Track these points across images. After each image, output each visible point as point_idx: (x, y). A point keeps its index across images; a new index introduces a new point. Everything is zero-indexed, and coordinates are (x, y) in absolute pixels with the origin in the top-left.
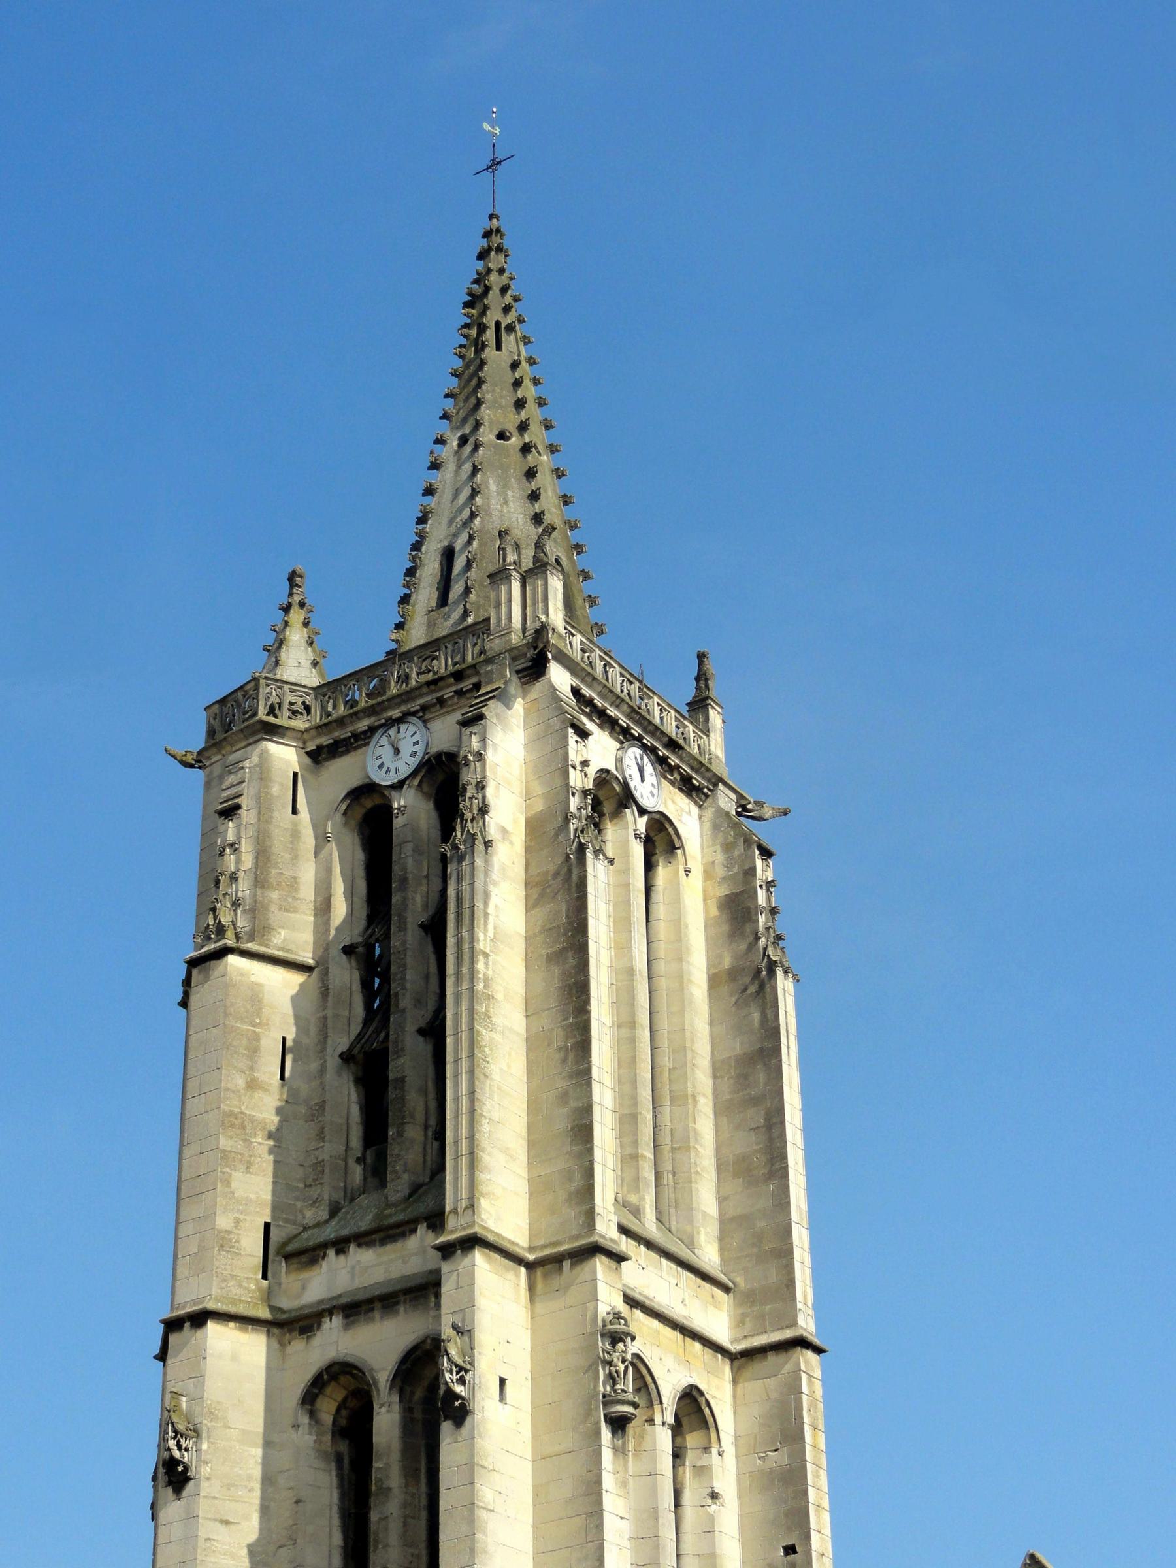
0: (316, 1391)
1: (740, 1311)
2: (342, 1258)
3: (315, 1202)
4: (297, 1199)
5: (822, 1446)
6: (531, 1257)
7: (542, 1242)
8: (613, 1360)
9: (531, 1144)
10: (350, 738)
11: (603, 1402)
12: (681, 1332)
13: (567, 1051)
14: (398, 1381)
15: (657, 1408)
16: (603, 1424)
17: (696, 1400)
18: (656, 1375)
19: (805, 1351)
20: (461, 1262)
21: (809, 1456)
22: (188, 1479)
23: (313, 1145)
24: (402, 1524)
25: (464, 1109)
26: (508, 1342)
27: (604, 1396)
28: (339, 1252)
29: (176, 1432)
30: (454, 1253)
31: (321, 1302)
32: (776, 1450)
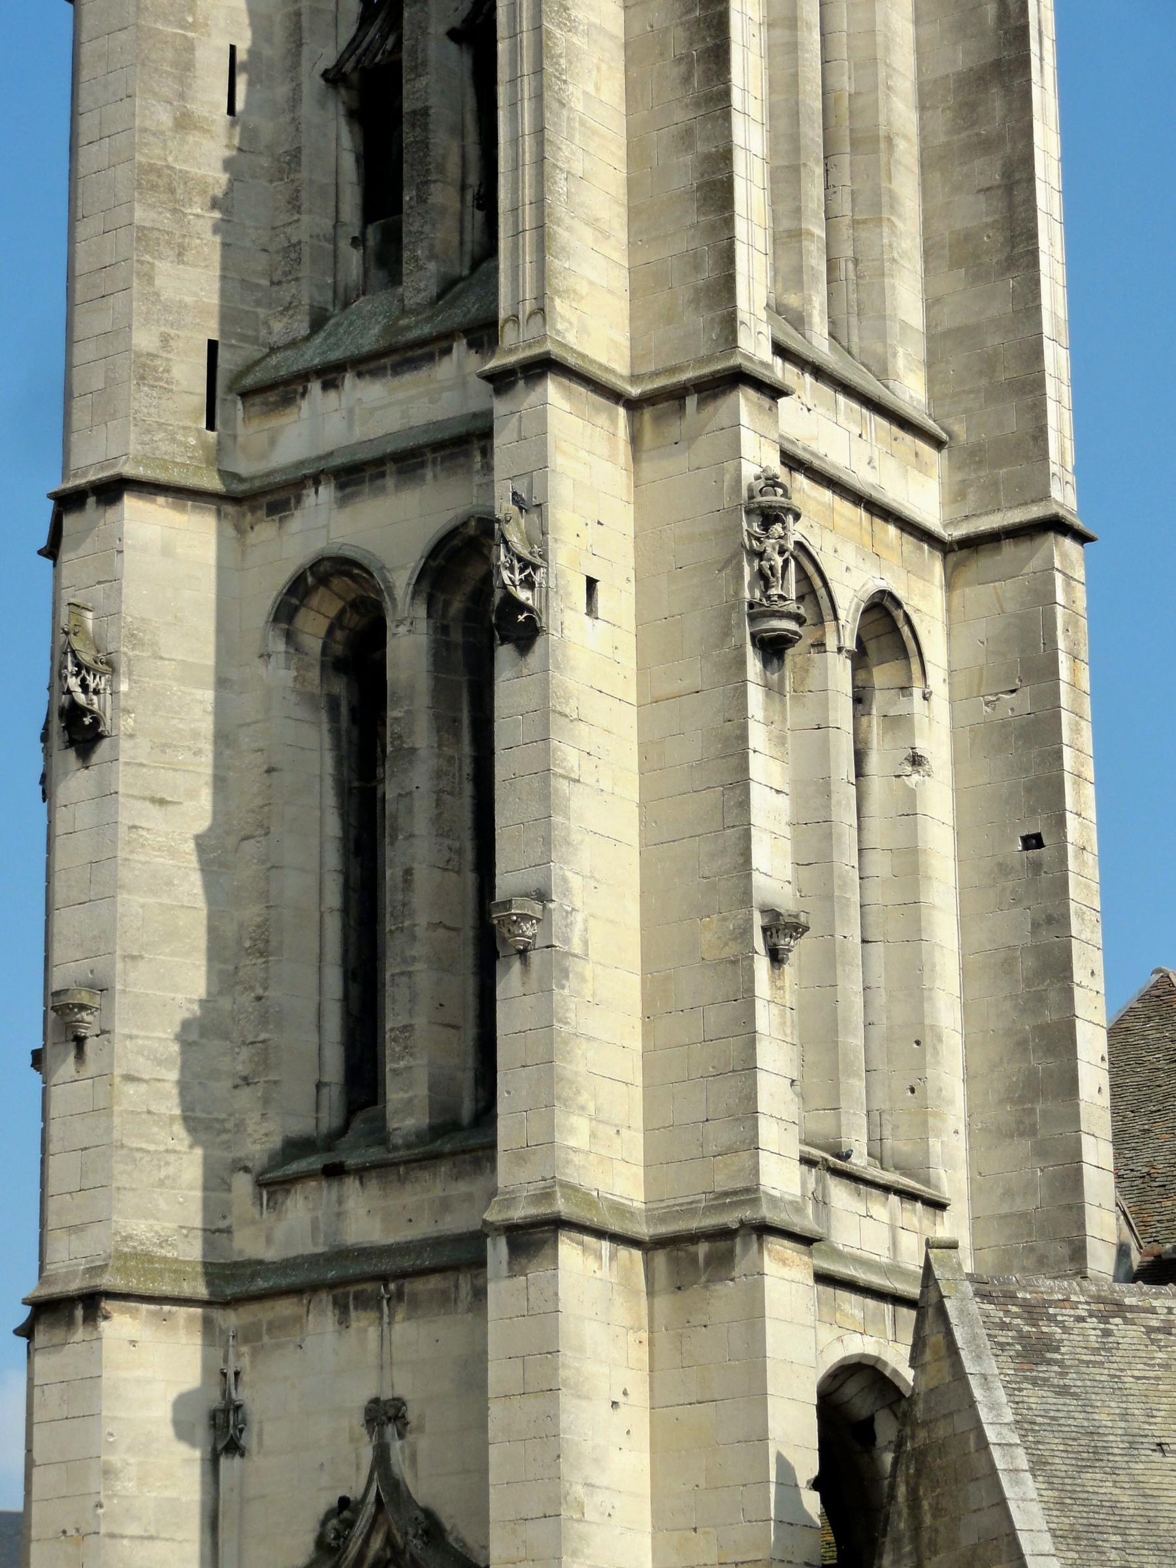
0: (295, 601)
1: (960, 476)
2: (332, 395)
3: (287, 309)
4: (258, 303)
5: (1086, 685)
6: (634, 391)
7: (652, 368)
8: (765, 550)
9: (634, 213)
11: (749, 615)
12: (867, 509)
13: (690, 65)
14: (425, 585)
15: (830, 626)
16: (749, 648)
17: (889, 614)
18: (828, 575)
19: (1061, 539)
20: (525, 399)
21: (1064, 700)
22: (100, 737)
23: (284, 218)
24: (434, 805)
25: (528, 157)
26: (599, 523)
27: (751, 606)
28: (327, 386)
29: (79, 665)
30: (514, 383)
31: (301, 464)
32: (1013, 691)
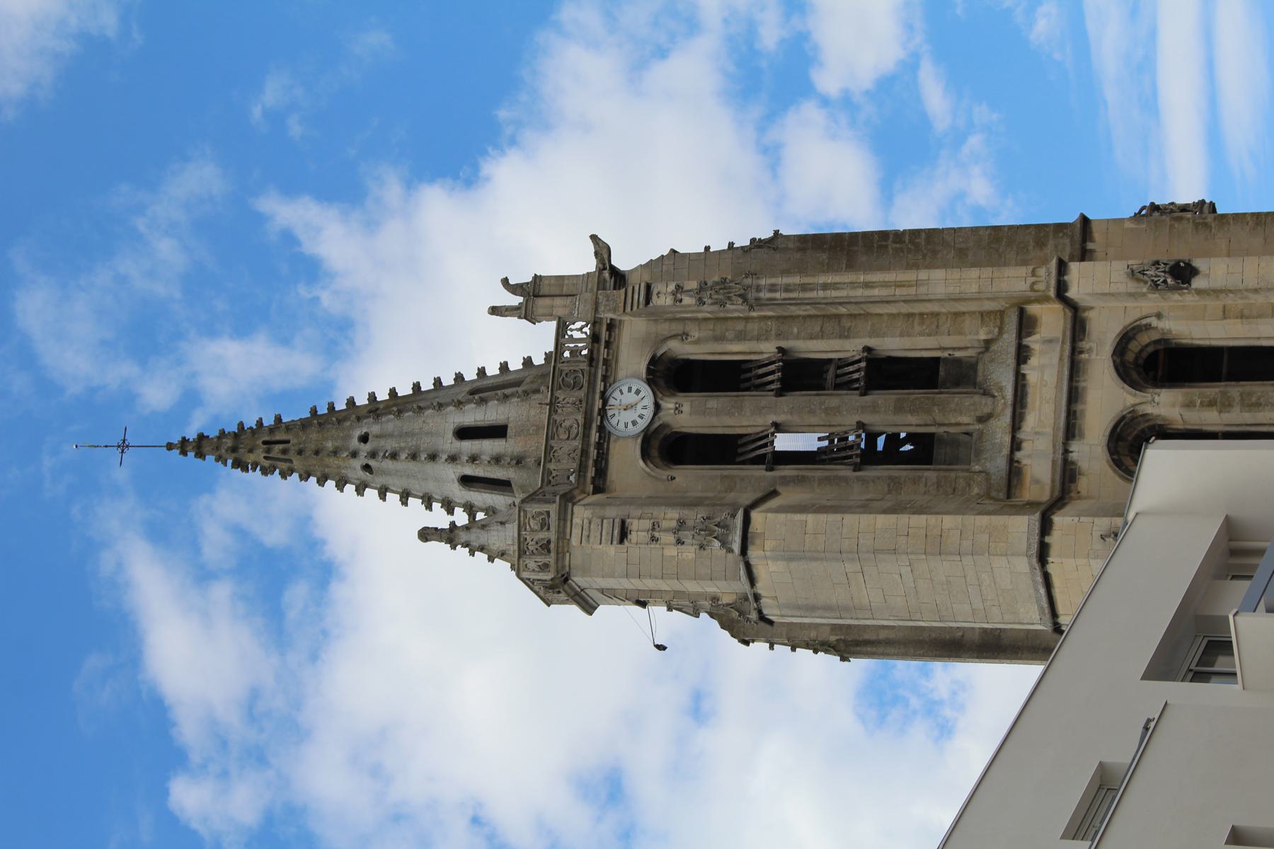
2: (1024, 445)
3: (969, 485)
10: (598, 453)
28: (1019, 449)
